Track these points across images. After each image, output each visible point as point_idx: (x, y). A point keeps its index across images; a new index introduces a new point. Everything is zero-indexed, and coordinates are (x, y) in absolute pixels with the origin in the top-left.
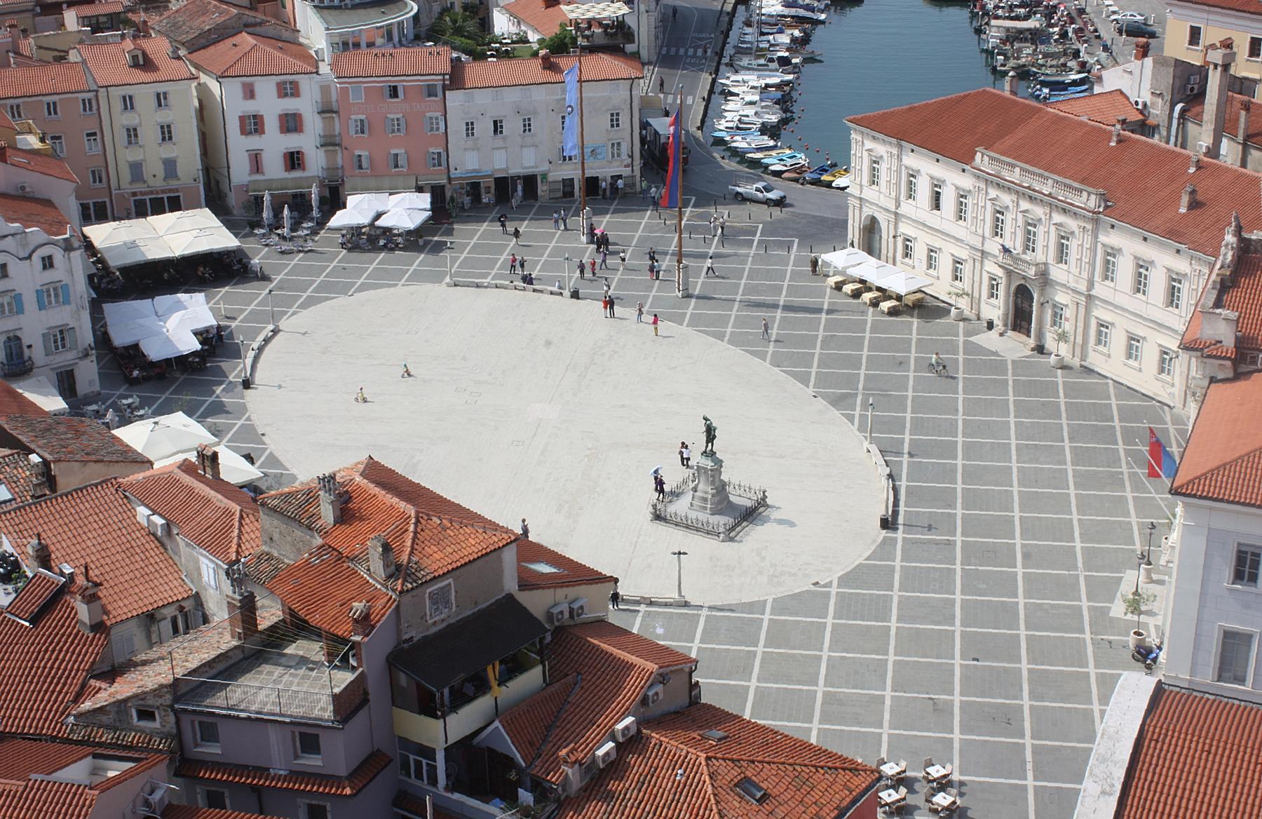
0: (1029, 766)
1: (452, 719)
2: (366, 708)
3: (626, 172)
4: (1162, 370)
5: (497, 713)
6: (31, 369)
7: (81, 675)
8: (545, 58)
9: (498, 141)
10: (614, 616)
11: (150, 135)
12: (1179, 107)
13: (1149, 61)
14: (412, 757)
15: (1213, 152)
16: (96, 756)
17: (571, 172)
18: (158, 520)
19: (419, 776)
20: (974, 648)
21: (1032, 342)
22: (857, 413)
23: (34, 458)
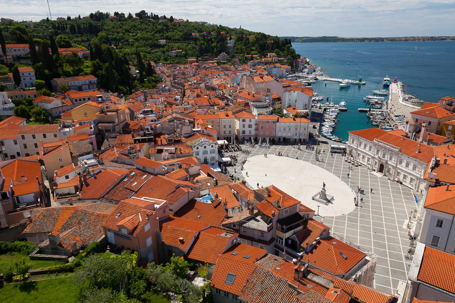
0: (388, 255)
1: (287, 233)
2: (272, 230)
3: (306, 138)
4: (411, 182)
5: (294, 233)
6: (208, 163)
7: (223, 218)
8: (294, 118)
9: (284, 131)
10: (314, 218)
11: (227, 127)
12: (414, 133)
13: (408, 125)
14: (279, 239)
15: (422, 142)
16: (226, 232)
17: (297, 138)
18: (236, 192)
19: (280, 243)
20: (375, 231)
21: (383, 174)
22: (350, 184)
23: (214, 179)
